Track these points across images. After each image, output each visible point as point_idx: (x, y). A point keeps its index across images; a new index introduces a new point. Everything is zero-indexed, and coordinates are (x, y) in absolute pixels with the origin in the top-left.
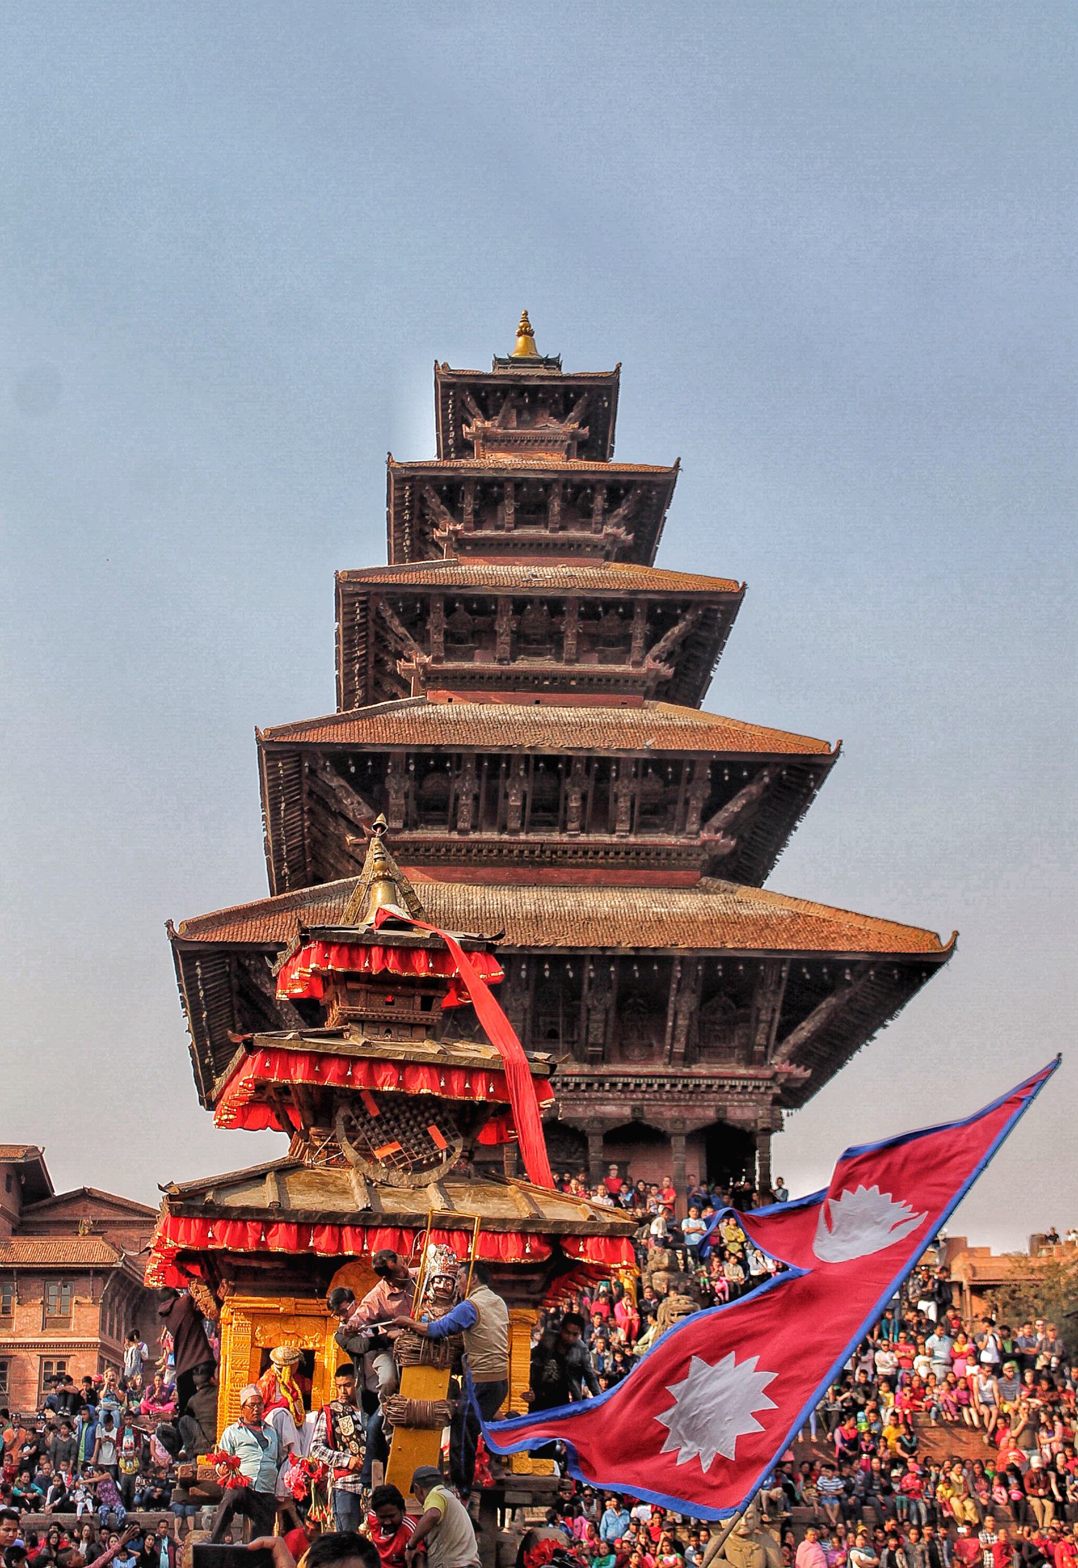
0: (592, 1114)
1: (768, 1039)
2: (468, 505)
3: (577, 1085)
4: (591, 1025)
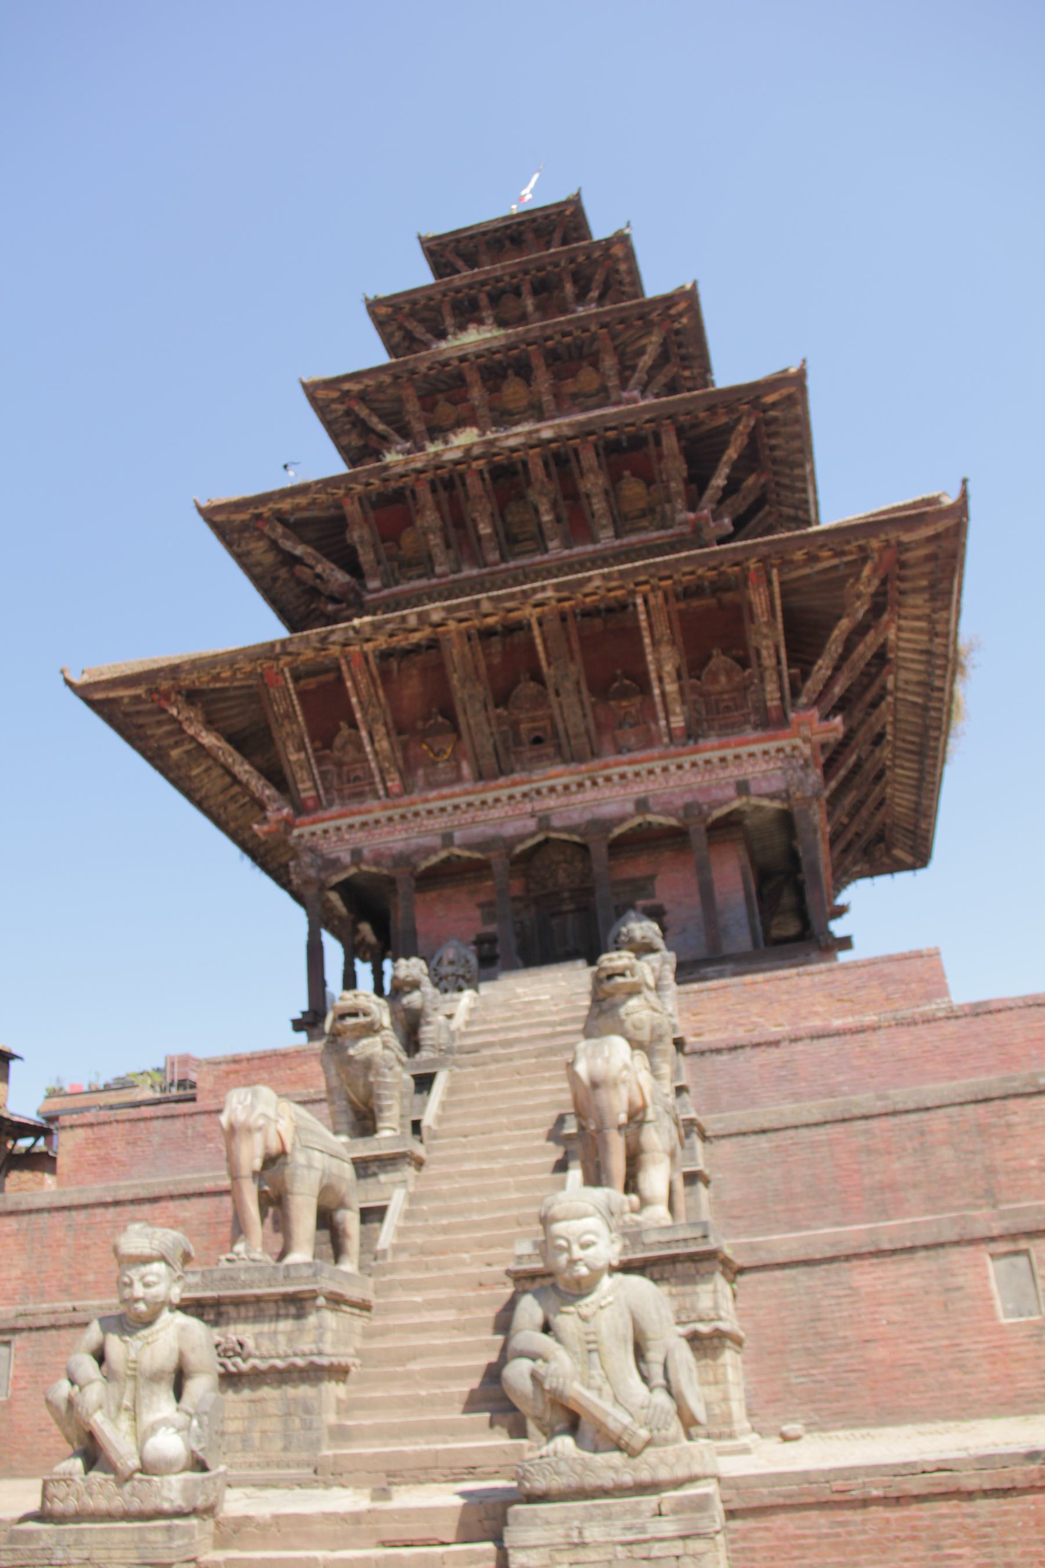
0: (587, 816)
1: (781, 689)
2: (449, 321)
3: (566, 787)
4: (566, 711)
